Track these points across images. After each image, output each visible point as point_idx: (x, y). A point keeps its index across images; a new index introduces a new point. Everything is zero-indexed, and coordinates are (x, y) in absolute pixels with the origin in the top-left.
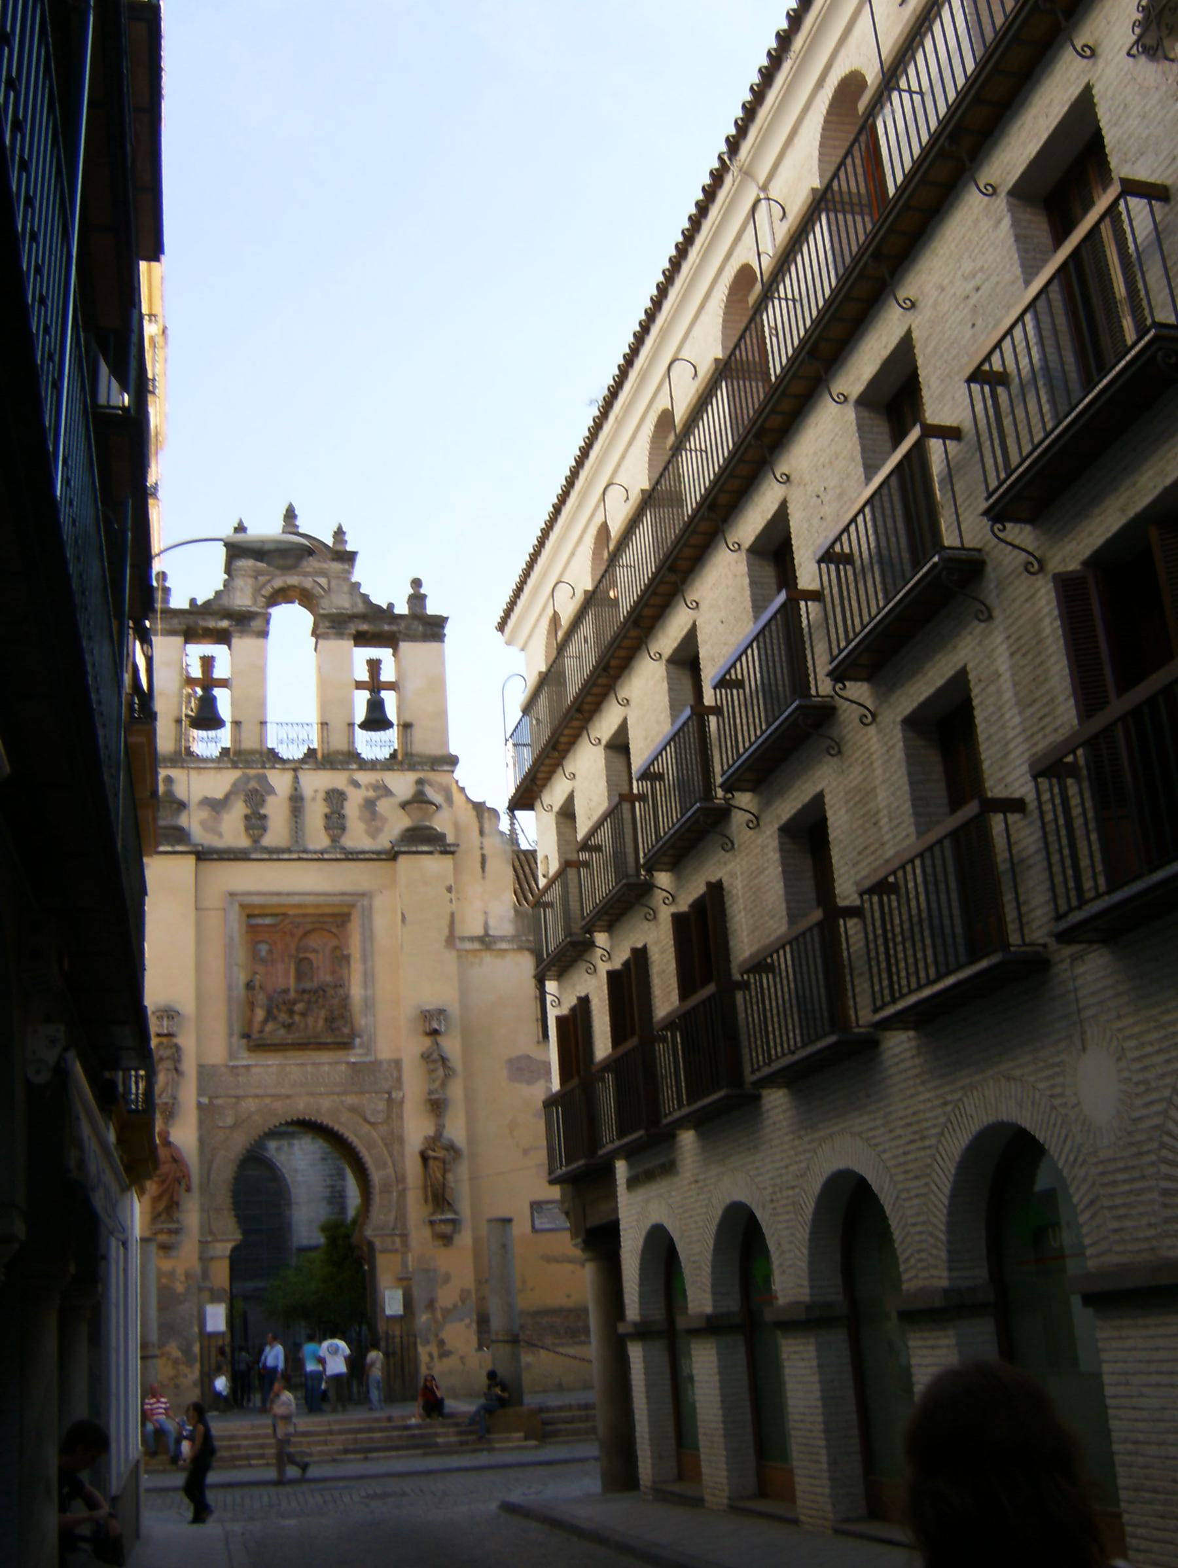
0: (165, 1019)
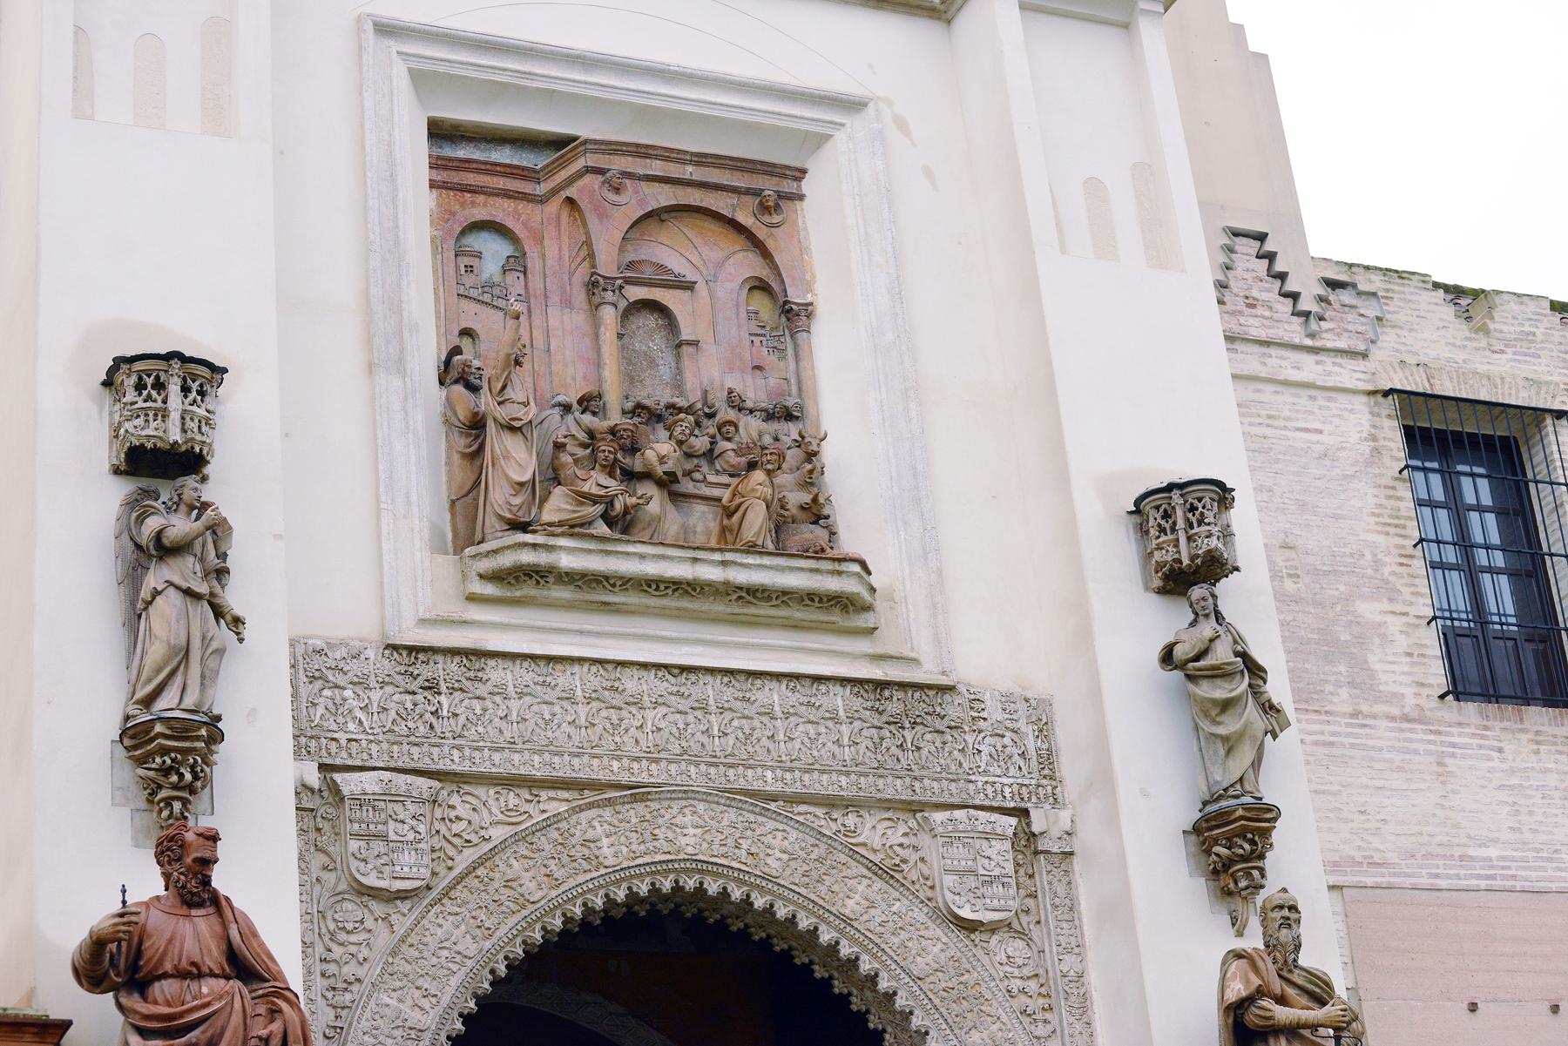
0: (174, 388)
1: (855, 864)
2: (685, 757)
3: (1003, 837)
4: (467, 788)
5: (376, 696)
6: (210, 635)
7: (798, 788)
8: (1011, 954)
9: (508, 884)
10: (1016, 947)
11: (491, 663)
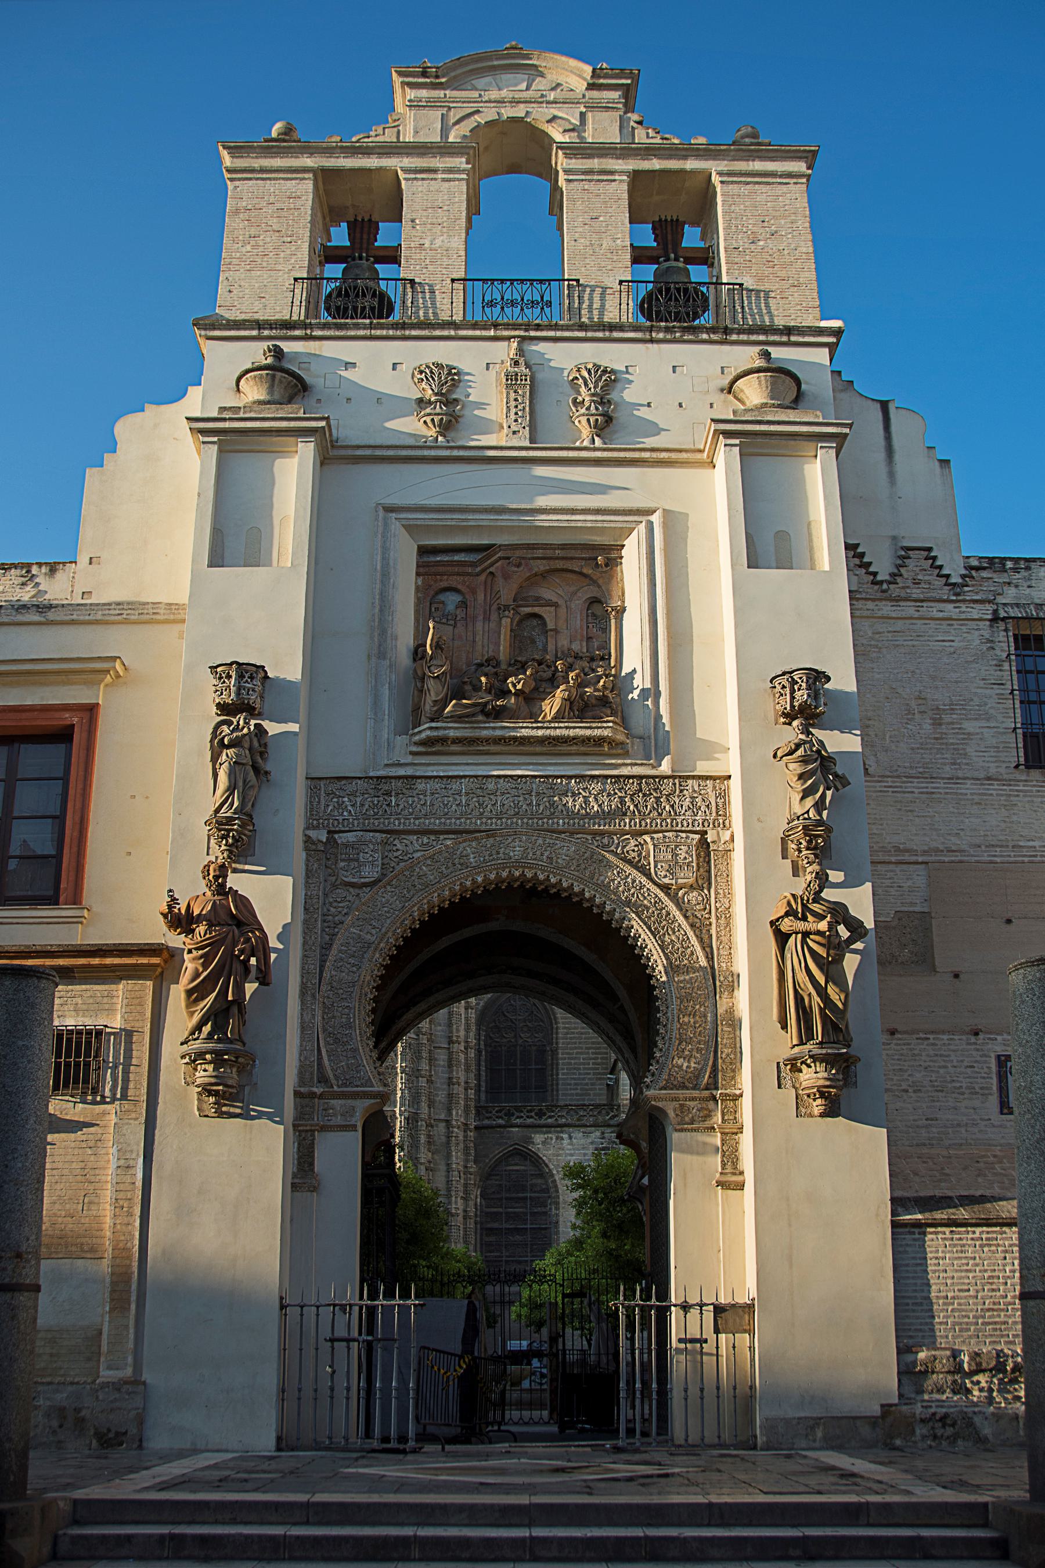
5: (359, 800)
9: (419, 877)
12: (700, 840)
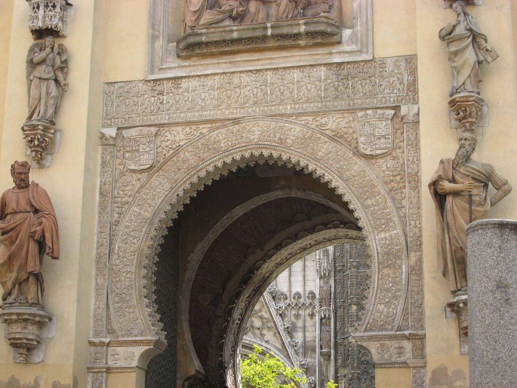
1: (323, 137)
2: (256, 105)
3: (387, 119)
4: (173, 128)
6: (50, 92)
7: (301, 111)
8: (389, 166)
9: (184, 162)
10: (390, 163)
11: (184, 81)
12: (395, 114)
